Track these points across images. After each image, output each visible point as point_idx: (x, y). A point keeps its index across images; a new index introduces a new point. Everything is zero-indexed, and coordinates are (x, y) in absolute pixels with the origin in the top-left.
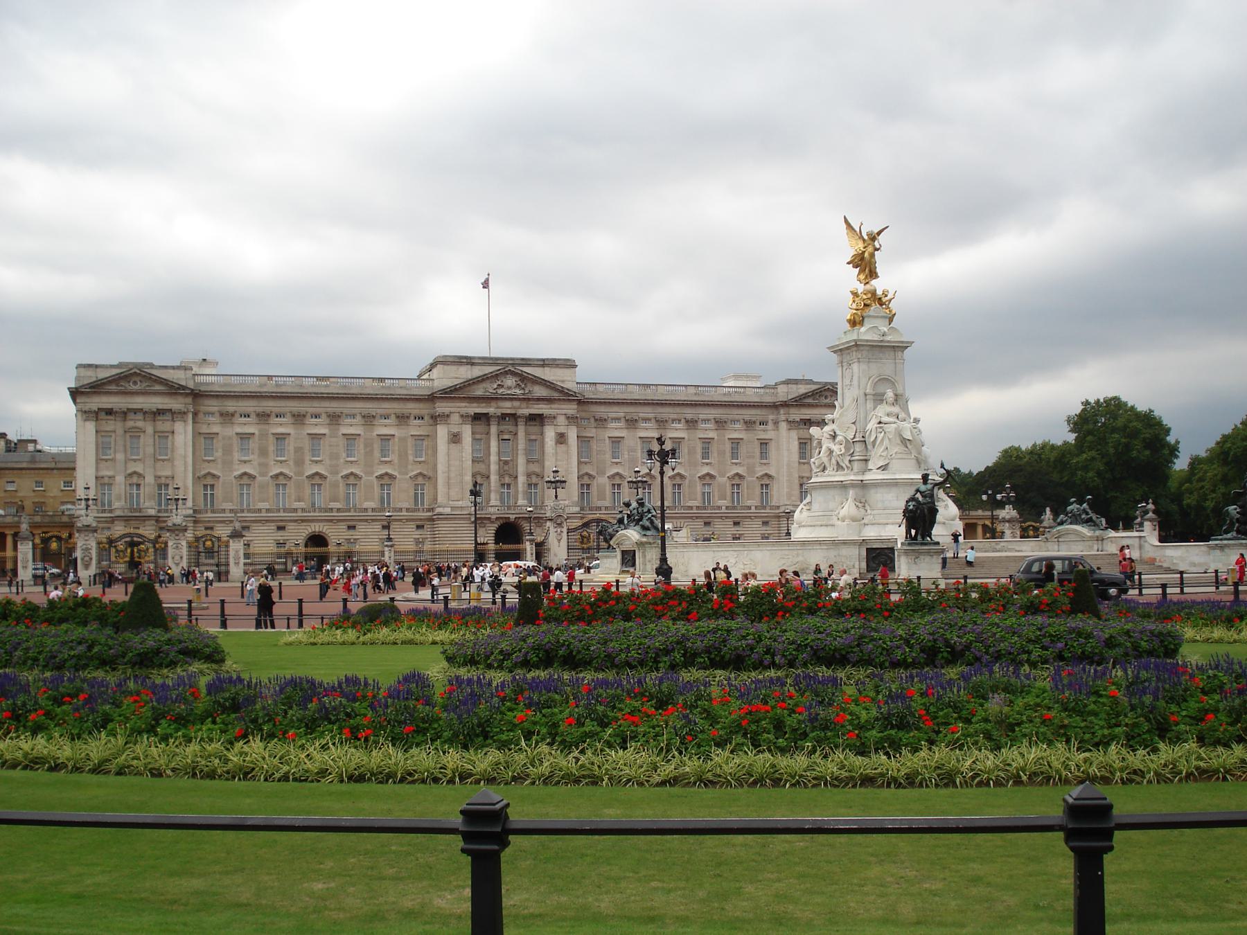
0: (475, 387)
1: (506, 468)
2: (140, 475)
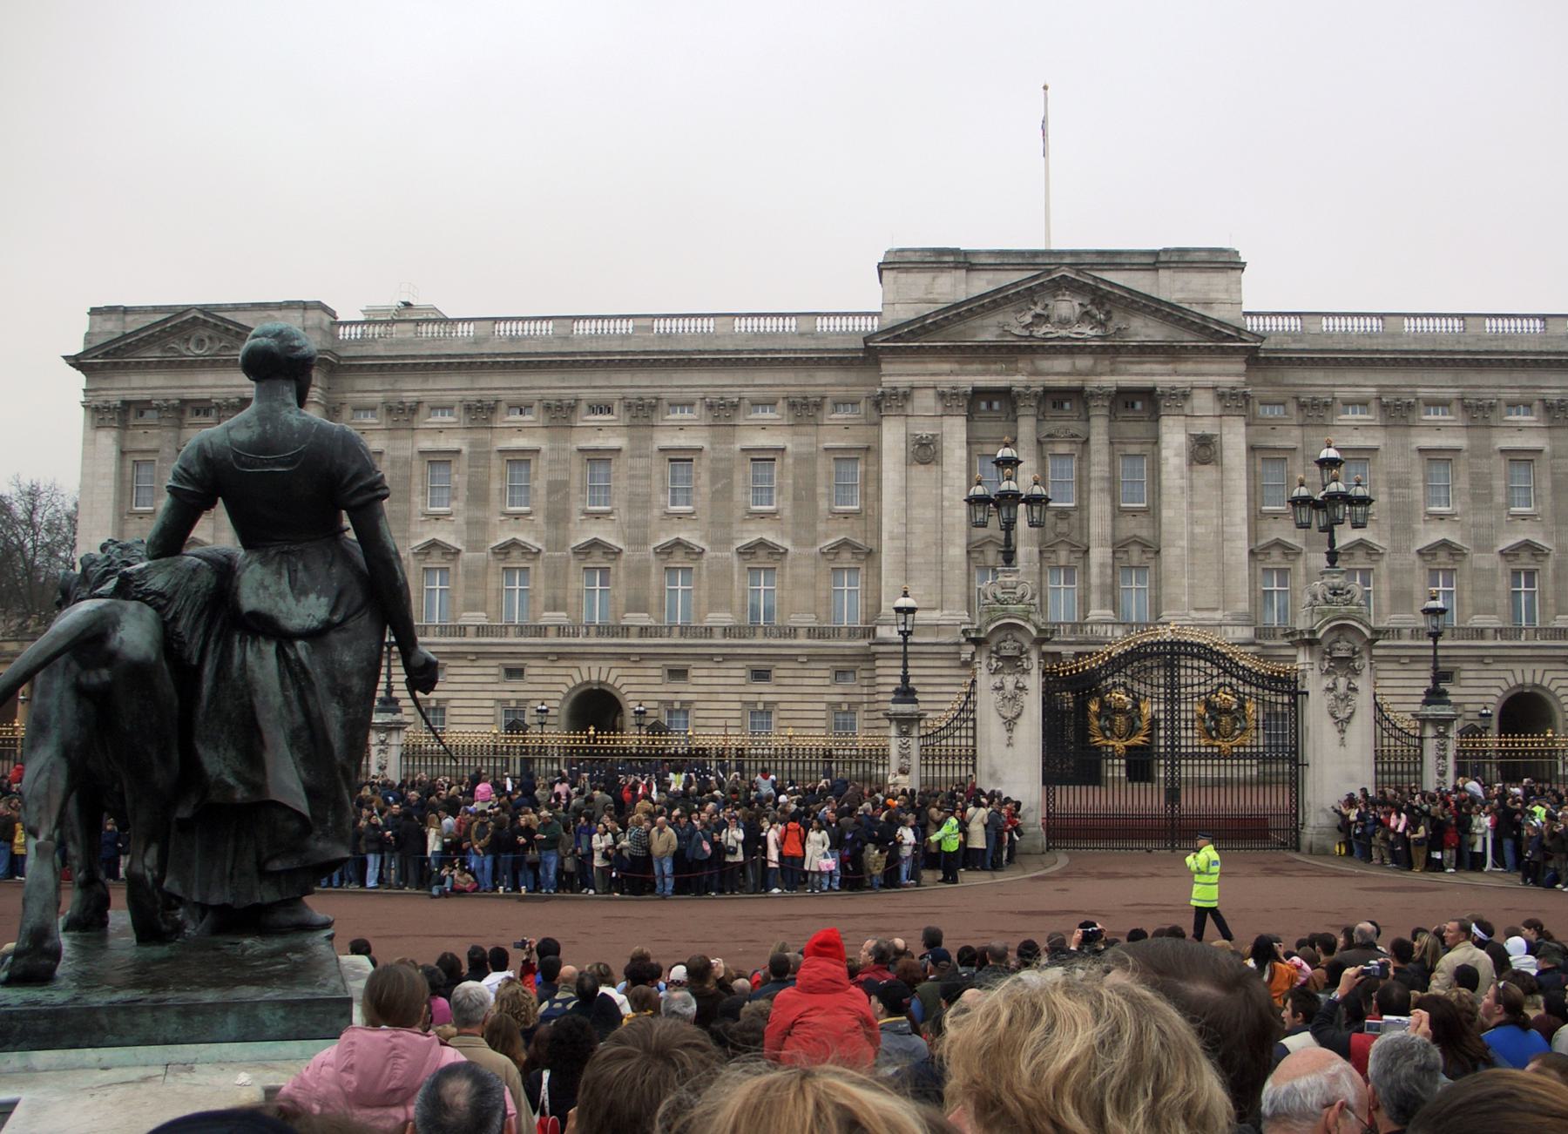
0: (976, 322)
1: (1062, 527)
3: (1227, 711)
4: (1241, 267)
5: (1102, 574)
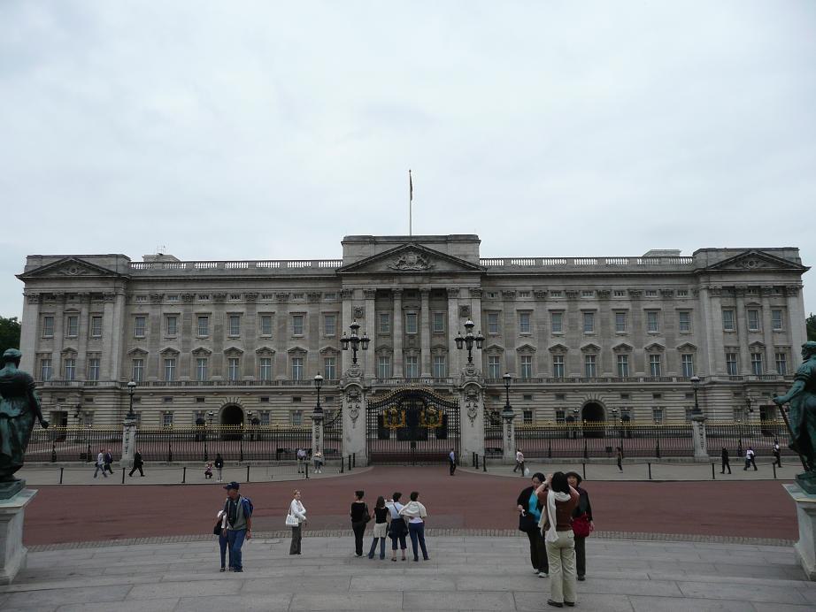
0: (379, 264)
1: (412, 341)
2: (74, 352)
3: (433, 415)
4: (479, 242)
5: (426, 359)
